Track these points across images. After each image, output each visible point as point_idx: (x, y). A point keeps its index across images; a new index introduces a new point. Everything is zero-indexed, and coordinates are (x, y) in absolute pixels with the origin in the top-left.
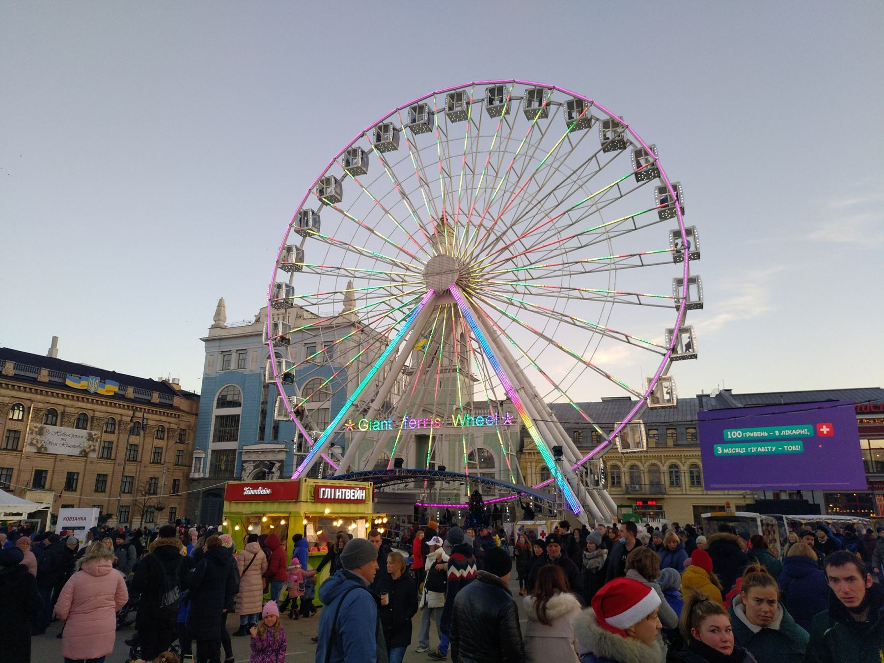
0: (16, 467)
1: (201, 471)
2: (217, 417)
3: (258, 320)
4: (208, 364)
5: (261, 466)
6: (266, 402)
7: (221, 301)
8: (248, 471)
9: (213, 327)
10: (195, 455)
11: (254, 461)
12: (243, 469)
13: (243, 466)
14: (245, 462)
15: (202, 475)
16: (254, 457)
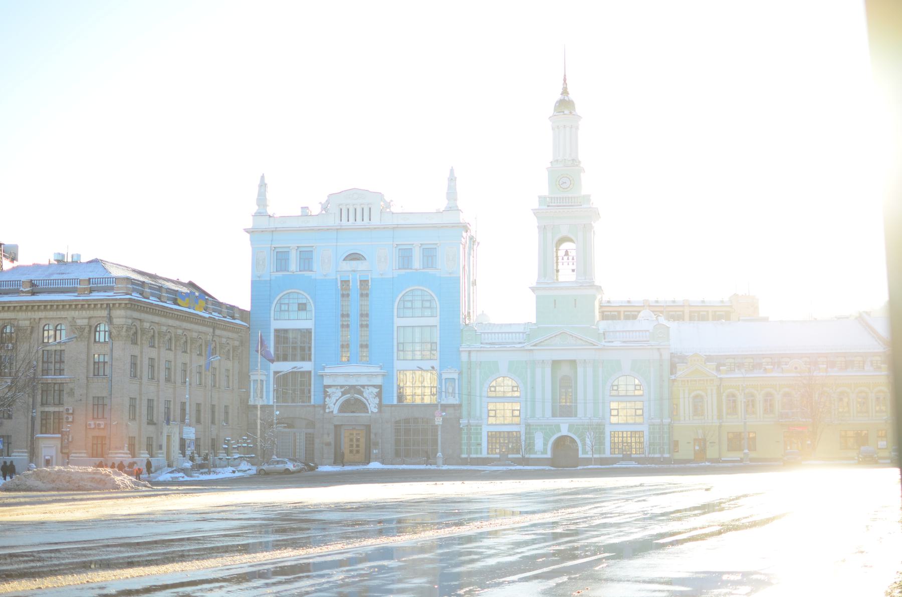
0: (155, 399)
1: (264, 395)
2: (276, 330)
3: (325, 208)
4: (257, 263)
5: (352, 391)
6: (348, 316)
7: (263, 177)
8: (334, 399)
9: (258, 215)
10: (252, 378)
11: (342, 387)
12: (326, 395)
13: (325, 392)
14: (330, 386)
15: (265, 403)
16: (341, 381)
